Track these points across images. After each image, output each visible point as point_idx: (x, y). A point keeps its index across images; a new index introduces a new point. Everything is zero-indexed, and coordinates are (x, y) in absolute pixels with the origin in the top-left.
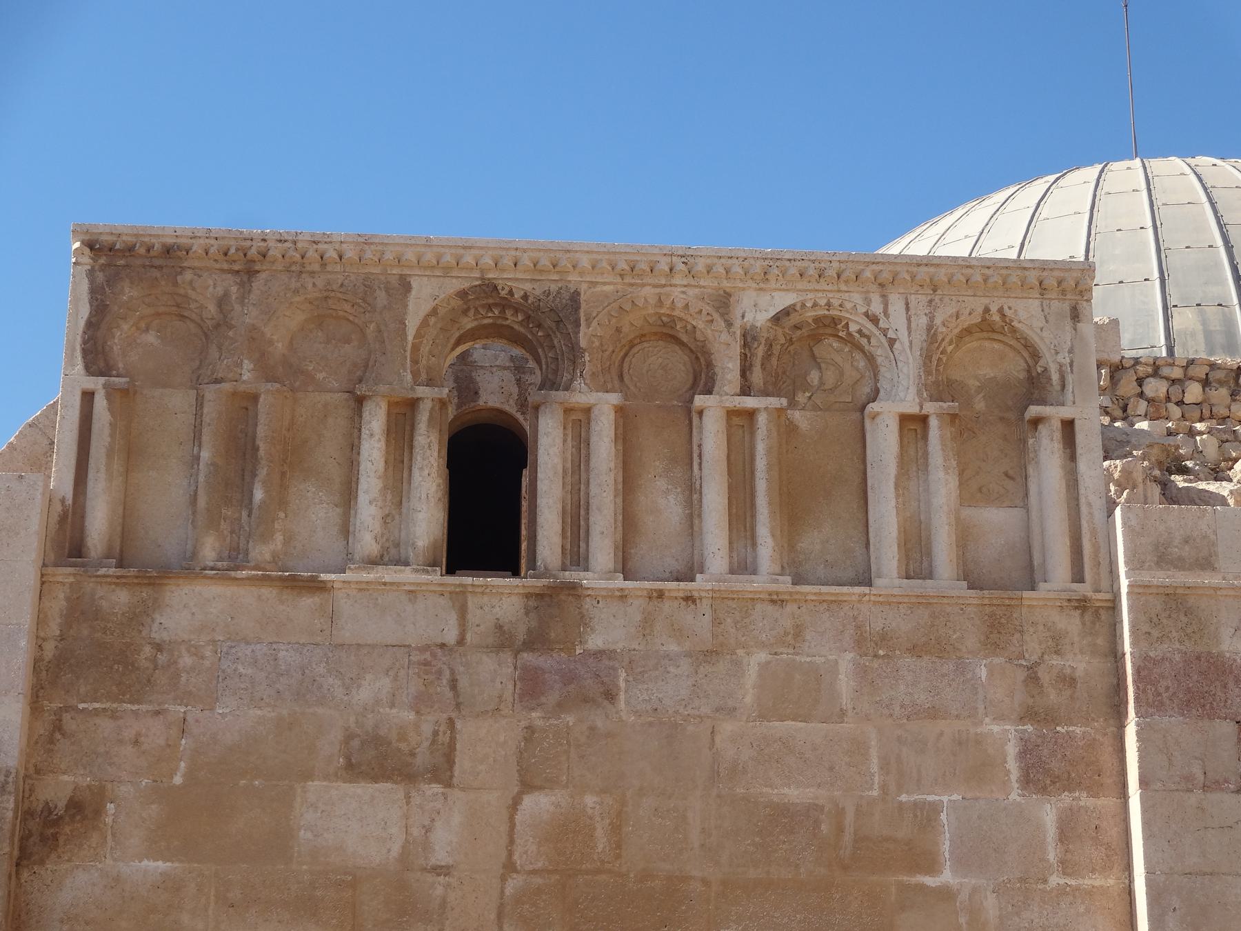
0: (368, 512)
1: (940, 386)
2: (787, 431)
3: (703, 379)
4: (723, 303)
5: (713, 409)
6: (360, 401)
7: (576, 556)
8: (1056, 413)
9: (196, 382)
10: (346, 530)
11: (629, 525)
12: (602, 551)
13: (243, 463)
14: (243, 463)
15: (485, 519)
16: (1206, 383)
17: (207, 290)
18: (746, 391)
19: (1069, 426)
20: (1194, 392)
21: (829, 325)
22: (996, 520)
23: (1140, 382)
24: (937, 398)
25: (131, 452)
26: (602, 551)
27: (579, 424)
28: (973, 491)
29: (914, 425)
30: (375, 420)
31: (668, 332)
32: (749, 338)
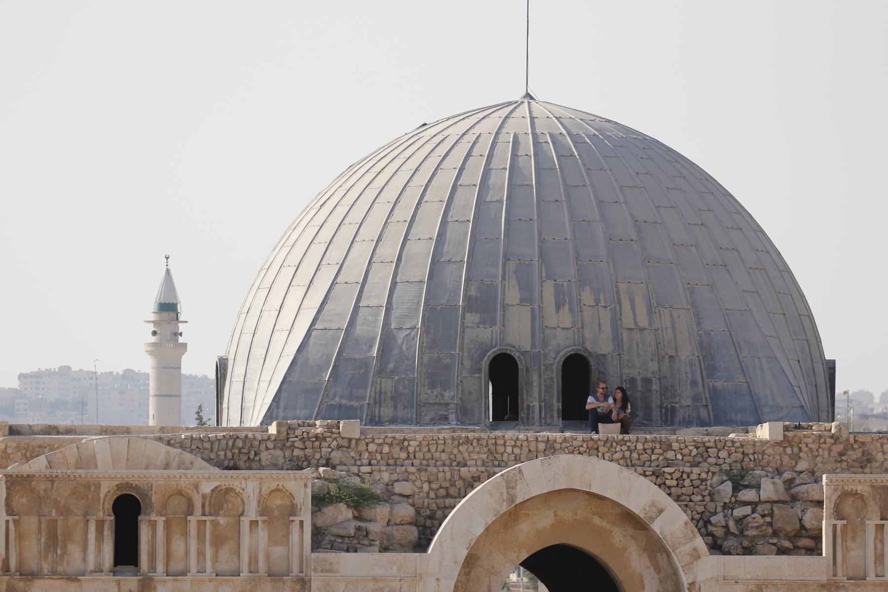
0: (91, 557)
1: (264, 511)
2: (215, 524)
3: (190, 511)
4: (196, 487)
5: (193, 520)
6: (88, 521)
7: (153, 568)
8: (297, 519)
9: (40, 515)
10: (84, 560)
11: (168, 556)
12: (160, 568)
13: (54, 540)
14: (54, 540)
15: (126, 553)
16: (391, 445)
17: (41, 487)
18: (204, 514)
19: (302, 522)
20: (386, 449)
21: (229, 490)
22: (278, 551)
23: (367, 445)
24: (262, 515)
25: (20, 537)
26: (160, 568)
27: (154, 525)
28: (273, 541)
29: (254, 524)
30: (92, 527)
31: (180, 493)
32: (204, 496)
